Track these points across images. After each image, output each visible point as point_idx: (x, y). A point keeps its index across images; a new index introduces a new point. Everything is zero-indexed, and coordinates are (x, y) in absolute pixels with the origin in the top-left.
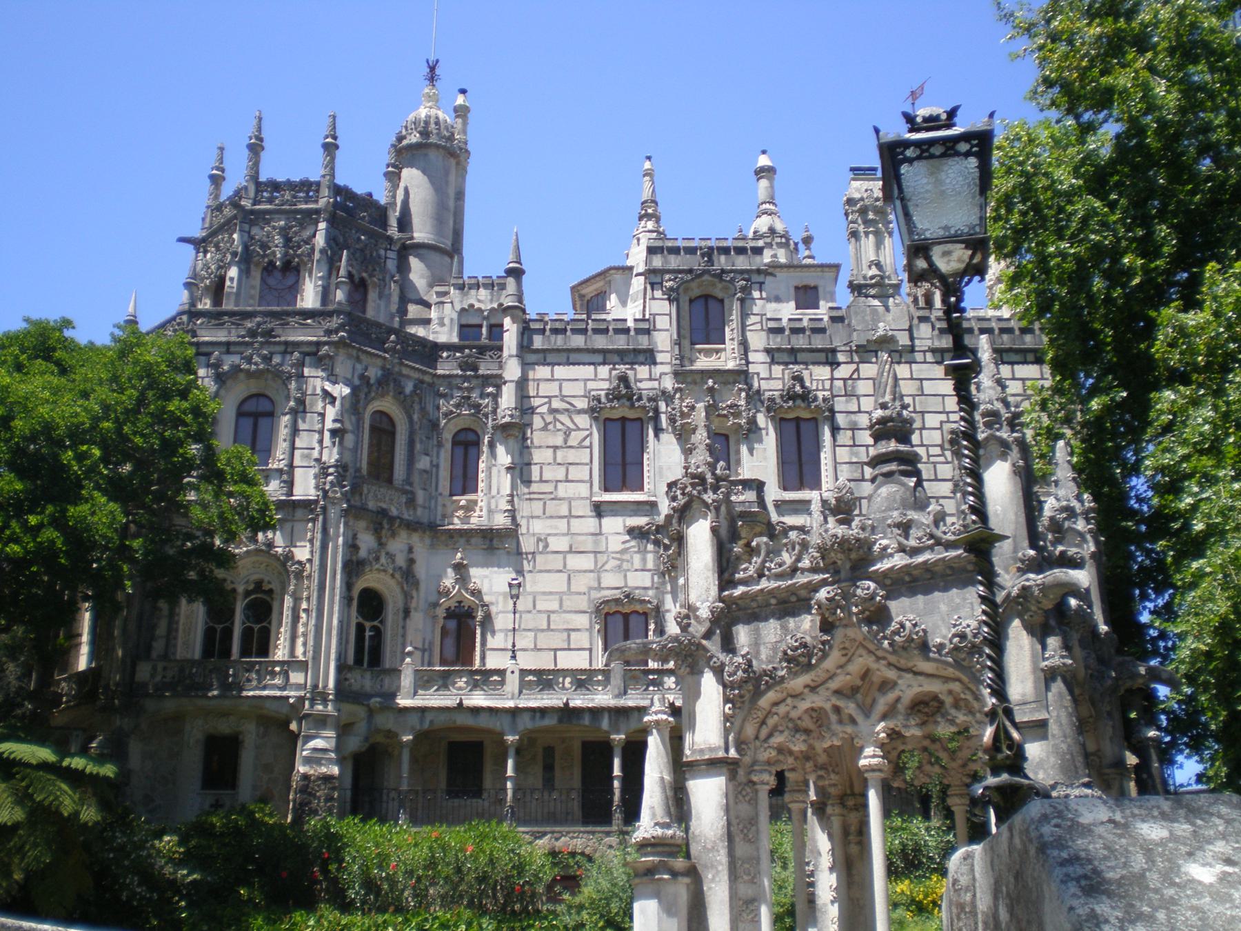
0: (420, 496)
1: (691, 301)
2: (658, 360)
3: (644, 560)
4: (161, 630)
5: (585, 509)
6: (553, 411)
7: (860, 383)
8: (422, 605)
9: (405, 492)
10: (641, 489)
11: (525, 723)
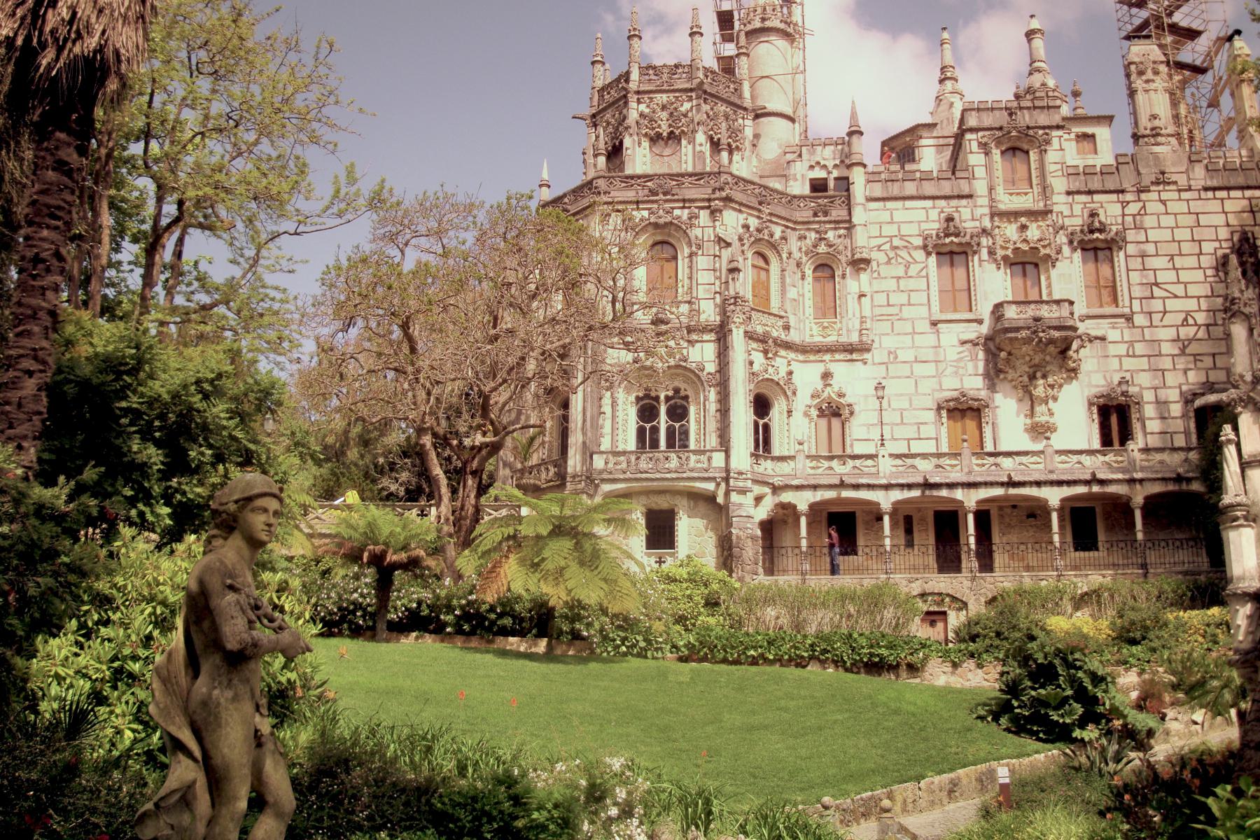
1: (1003, 153)
2: (979, 203)
3: (976, 367)
4: (607, 428)
5: (924, 326)
6: (895, 248)
7: (1146, 217)
9: (781, 317)
10: (971, 310)
11: (897, 495)
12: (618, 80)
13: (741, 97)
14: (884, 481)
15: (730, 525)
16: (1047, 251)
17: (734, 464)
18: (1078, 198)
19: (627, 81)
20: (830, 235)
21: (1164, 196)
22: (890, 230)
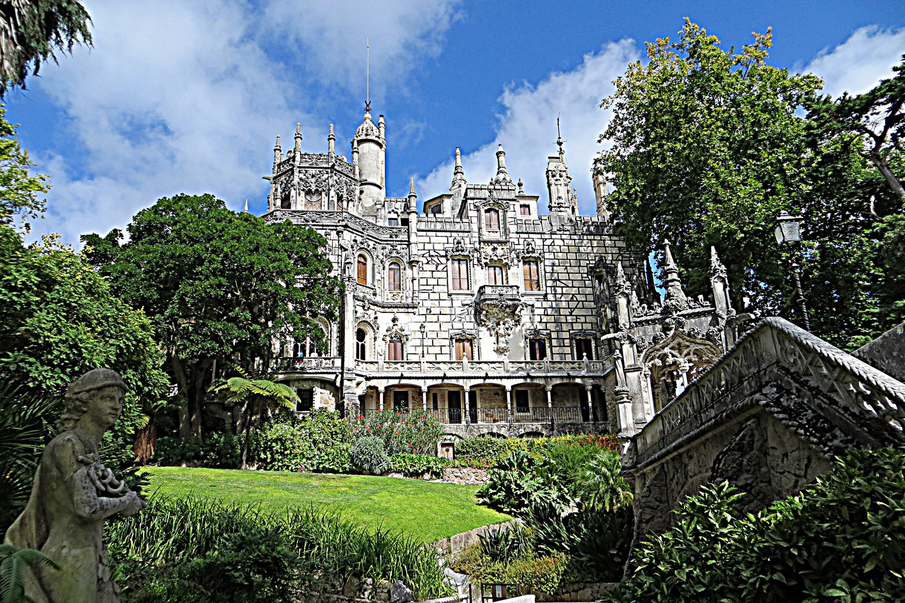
5: (445, 296)
6: (430, 256)
8: (382, 337)
11: (430, 382)
12: (289, 160)
13: (354, 174)
14: (423, 375)
16: (506, 261)
17: (346, 365)
18: (522, 236)
19: (294, 161)
20: (398, 247)
21: (563, 237)
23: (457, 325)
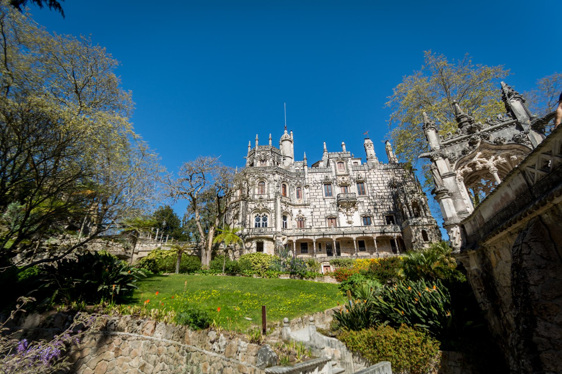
0: (292, 199)
5: (322, 200)
11: (317, 237)
15: (276, 245)
22: (313, 180)
23: (328, 212)
